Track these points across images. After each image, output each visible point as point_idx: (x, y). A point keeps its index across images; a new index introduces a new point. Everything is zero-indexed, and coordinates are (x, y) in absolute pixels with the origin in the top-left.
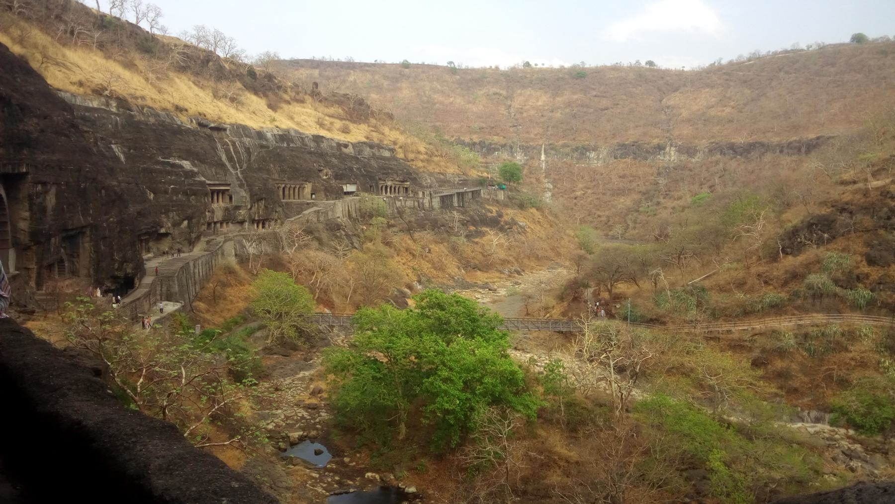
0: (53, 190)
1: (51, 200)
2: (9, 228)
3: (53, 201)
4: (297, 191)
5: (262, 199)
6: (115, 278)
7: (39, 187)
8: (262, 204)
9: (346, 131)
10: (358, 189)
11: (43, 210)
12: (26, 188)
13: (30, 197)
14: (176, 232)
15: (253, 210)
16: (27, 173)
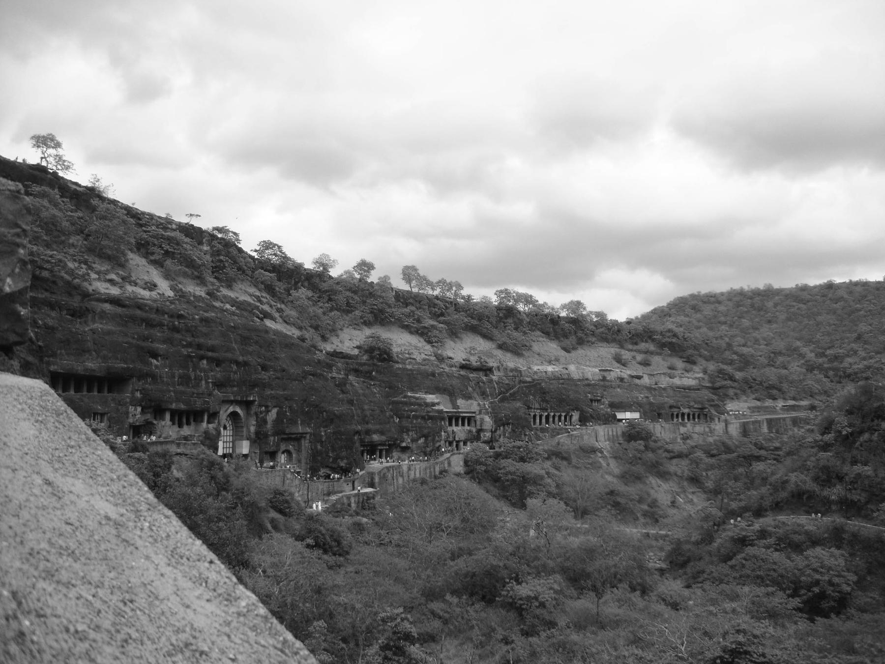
2: (245, 429)
3: (275, 416)
4: (563, 418)
5: (508, 424)
7: (263, 408)
8: (509, 429)
9: (645, 364)
10: (641, 417)
11: (265, 422)
12: (254, 409)
13: (256, 414)
14: (414, 446)
15: (498, 432)
16: (254, 401)
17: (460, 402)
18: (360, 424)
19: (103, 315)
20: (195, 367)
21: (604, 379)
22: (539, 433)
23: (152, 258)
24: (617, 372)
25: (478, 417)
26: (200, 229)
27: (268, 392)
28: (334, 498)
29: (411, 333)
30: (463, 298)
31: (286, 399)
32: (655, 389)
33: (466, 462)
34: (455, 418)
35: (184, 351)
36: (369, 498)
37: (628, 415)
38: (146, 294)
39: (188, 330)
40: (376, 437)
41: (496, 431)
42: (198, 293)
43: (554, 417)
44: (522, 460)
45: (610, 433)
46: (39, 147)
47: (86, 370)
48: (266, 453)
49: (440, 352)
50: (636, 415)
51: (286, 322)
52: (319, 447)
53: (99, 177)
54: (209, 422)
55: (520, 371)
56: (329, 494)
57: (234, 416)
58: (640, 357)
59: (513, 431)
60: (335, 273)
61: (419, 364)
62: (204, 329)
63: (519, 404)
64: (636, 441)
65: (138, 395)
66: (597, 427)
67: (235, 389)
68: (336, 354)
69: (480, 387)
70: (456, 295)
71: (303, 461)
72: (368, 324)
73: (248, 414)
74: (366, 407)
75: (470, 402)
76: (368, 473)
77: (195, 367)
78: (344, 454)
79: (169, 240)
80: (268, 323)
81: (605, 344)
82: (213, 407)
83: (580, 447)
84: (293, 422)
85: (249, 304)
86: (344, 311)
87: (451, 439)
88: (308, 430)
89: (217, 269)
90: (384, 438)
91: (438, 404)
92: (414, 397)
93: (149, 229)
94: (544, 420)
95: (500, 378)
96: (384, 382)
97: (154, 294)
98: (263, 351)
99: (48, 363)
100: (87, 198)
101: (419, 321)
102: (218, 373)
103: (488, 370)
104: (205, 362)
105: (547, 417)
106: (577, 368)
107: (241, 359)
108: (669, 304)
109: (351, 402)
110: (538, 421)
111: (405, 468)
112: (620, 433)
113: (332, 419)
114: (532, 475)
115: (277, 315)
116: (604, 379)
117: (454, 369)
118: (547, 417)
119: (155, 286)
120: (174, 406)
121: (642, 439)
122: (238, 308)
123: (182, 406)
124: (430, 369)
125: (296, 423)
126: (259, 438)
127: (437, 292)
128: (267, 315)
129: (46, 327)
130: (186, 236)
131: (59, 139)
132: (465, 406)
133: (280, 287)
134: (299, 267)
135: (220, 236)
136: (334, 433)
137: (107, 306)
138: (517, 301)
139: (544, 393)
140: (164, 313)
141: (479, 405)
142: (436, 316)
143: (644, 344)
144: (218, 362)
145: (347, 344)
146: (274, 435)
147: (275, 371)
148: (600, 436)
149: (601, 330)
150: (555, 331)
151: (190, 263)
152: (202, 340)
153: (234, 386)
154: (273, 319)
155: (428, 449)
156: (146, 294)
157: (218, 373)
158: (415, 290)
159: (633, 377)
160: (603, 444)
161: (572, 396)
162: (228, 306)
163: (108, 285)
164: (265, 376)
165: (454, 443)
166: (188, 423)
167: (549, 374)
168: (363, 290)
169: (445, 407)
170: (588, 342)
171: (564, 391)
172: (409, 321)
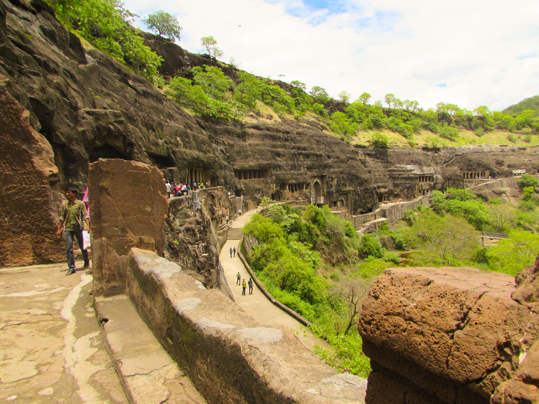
0: (335, 180)
1: (335, 182)
5: (451, 179)
6: (364, 209)
9: (528, 141)
10: (527, 172)
11: (331, 186)
12: (326, 179)
13: (327, 182)
15: (446, 184)
17: (425, 168)
18: (374, 183)
19: (252, 135)
20: (298, 160)
21: (503, 151)
22: (467, 183)
23: (266, 101)
24: (511, 145)
25: (434, 176)
26: (285, 83)
27: (332, 170)
28: (367, 224)
29: (393, 131)
30: (418, 110)
31: (341, 173)
32: (535, 155)
33: (430, 202)
34: (423, 178)
35: (292, 151)
36: (385, 224)
37: (519, 171)
38: (268, 121)
39: (292, 140)
40: (382, 190)
41: (444, 183)
42: (291, 119)
43: (475, 174)
44: (462, 199)
45: (510, 182)
46: (205, 44)
47: (250, 166)
48: (332, 202)
49: (411, 141)
50: (524, 171)
51: (333, 131)
52: (357, 198)
53: (234, 58)
54: (306, 189)
55: (455, 149)
56: (364, 223)
57: (317, 183)
58: (523, 137)
59: (454, 183)
60: (351, 101)
61: (401, 148)
62: (298, 138)
63: (456, 168)
64: (528, 187)
65: (274, 177)
66: (502, 179)
67: (317, 170)
68: (357, 146)
69: (434, 160)
70: (415, 108)
71: (349, 205)
72: (370, 128)
73: (322, 182)
74: (376, 174)
75: (430, 168)
76: (382, 210)
77: (298, 160)
78: (369, 201)
79: (273, 91)
80: (325, 132)
81: (501, 131)
82: (309, 180)
83: (493, 191)
84: (344, 185)
85: (315, 123)
86: (358, 122)
87: (420, 189)
88: (352, 189)
89: (297, 104)
90: (386, 190)
91: (413, 170)
92: (400, 167)
93: (262, 85)
94: (469, 176)
95: (444, 153)
96: (384, 160)
97: (272, 121)
98: (327, 148)
99: (233, 165)
100: (230, 71)
101: (397, 125)
102: (308, 162)
103: (436, 150)
104: (301, 156)
105: (471, 174)
106: (487, 145)
107: (318, 153)
108: (520, 103)
109: (370, 172)
110: (466, 177)
111: (400, 206)
112: (516, 182)
113: (362, 182)
114: (472, 209)
115: (327, 127)
116: (503, 151)
117: (419, 150)
118: (471, 174)
119: (272, 117)
120: (290, 182)
121: (531, 186)
122: (310, 125)
123: (294, 181)
124: (407, 151)
126: (329, 195)
127: (404, 107)
128: (324, 128)
129: (229, 145)
130: (281, 87)
131: (215, 39)
132: (427, 170)
133: (326, 111)
134: (332, 100)
135: (295, 86)
136: (364, 190)
138: (448, 109)
139: (470, 161)
140: (280, 131)
141: (434, 169)
142: (405, 121)
143: (524, 129)
144: (307, 156)
145: (362, 140)
146: (336, 192)
147: (334, 158)
148: (503, 185)
149: (497, 122)
150: (470, 124)
151: (284, 102)
152: (299, 145)
153: (316, 168)
154: (326, 129)
155: (409, 195)
156: (268, 121)
157: (308, 162)
158: (392, 107)
159: (520, 149)
160: (507, 189)
161: (485, 161)
162: (305, 125)
163: (250, 118)
164: (330, 161)
165: (423, 192)
166: (296, 190)
167: (471, 149)
168: (366, 110)
169: (417, 171)
170: (490, 129)
171: (480, 159)
172: (392, 125)
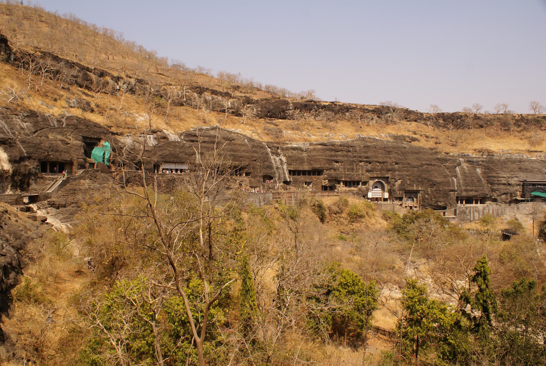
0: (399, 182)
14: (498, 198)
27: (397, 173)
77: (357, 165)
120: (343, 179)
123: (348, 179)
125: (413, 186)
128: (414, 140)
137: (320, 146)
